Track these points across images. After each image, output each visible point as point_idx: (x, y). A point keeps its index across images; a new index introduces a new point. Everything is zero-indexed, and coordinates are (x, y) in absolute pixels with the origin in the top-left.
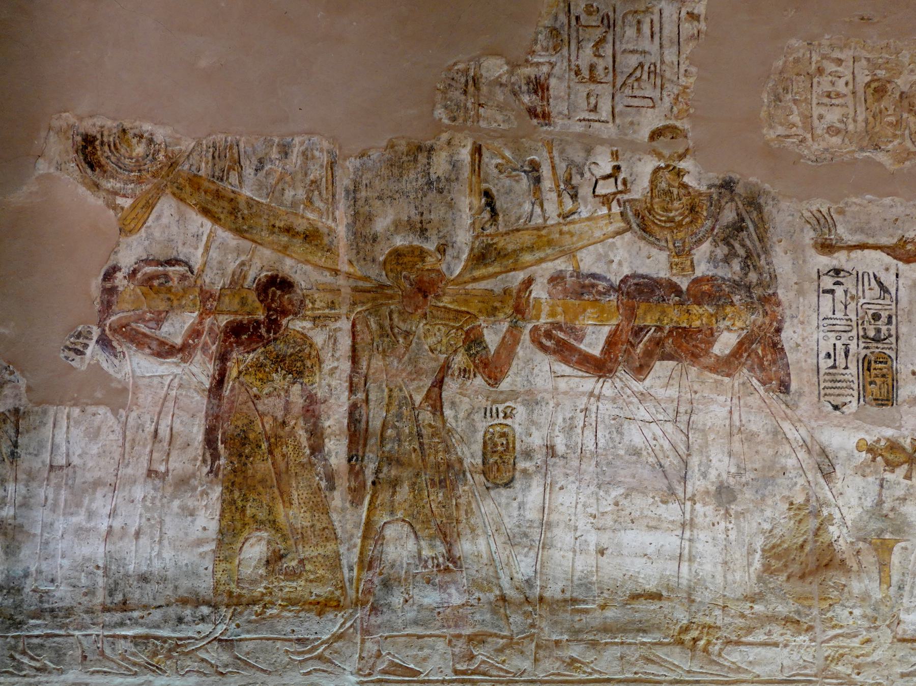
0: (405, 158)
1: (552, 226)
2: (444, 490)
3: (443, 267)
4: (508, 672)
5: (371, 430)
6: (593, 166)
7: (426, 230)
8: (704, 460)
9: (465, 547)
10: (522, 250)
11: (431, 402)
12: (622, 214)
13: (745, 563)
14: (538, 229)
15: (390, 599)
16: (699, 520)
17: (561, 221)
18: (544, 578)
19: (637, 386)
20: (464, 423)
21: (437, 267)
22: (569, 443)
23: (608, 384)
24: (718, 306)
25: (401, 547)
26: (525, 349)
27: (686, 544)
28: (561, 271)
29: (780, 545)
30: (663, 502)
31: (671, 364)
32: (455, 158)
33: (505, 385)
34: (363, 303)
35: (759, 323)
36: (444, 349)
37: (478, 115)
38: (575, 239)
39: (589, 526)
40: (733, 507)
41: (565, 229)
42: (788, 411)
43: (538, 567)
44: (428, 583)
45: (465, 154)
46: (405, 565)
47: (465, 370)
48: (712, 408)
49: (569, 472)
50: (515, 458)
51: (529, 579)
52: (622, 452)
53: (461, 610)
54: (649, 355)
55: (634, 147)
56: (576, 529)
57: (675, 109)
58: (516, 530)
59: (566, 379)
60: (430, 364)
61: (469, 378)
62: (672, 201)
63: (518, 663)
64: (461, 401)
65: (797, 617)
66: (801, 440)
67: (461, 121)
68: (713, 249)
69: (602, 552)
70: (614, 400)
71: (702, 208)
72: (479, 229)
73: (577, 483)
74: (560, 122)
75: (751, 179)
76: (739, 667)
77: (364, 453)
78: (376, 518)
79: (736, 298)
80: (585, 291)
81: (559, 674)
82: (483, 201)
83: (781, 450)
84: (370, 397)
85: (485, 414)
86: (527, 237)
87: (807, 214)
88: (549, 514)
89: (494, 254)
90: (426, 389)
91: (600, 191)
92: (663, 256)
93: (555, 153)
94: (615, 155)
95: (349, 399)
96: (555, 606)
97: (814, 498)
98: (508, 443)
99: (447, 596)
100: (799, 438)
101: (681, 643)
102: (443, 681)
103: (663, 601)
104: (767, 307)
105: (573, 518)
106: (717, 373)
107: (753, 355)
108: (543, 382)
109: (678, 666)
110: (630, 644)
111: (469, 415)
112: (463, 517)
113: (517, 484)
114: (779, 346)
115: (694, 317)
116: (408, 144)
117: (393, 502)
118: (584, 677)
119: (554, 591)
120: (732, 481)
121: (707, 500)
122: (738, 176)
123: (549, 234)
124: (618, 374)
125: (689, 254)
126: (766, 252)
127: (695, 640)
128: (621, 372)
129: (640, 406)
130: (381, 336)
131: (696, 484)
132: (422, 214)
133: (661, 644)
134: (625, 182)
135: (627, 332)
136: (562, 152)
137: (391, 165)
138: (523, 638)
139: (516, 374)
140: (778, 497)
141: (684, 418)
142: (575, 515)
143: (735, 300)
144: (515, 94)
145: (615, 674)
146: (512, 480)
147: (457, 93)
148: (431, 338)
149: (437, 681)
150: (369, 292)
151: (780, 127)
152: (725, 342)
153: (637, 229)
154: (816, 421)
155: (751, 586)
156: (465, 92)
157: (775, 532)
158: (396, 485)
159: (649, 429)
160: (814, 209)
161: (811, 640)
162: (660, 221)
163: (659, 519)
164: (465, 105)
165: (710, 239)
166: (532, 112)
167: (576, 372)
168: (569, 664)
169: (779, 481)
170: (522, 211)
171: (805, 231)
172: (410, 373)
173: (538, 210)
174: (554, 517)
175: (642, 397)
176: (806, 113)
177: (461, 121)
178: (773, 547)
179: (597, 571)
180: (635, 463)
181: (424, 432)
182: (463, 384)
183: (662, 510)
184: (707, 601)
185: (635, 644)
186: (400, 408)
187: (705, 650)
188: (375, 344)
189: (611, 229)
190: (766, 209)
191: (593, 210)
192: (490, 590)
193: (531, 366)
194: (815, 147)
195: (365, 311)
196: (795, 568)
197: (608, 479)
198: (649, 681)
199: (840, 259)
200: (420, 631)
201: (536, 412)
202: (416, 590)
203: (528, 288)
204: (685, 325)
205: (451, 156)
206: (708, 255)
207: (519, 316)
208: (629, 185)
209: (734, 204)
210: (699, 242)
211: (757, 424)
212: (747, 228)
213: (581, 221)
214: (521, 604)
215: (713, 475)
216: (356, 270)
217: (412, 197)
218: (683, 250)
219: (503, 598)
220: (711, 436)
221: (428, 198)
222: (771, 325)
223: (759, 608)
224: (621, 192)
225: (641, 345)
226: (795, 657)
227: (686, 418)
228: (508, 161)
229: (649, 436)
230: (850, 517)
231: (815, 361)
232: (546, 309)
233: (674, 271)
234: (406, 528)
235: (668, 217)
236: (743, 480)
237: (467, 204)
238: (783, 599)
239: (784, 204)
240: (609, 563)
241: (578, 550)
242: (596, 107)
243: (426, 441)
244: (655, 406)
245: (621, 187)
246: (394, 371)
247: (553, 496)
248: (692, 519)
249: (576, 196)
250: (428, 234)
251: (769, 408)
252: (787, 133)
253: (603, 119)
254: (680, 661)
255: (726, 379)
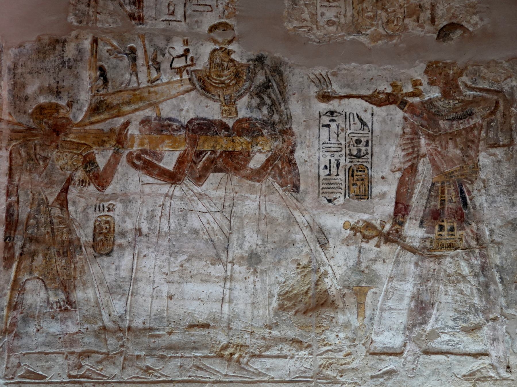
0: (47, 47)
1: (144, 88)
2: (66, 258)
3: (71, 116)
4: (104, 376)
5: (20, 220)
6: (171, 49)
7: (60, 92)
8: (241, 236)
9: (78, 295)
10: (123, 103)
11: (60, 202)
12: (190, 79)
13: (267, 303)
14: (134, 90)
15: (28, 329)
16: (236, 276)
17: (149, 84)
18: (132, 314)
19: (198, 189)
20: (81, 215)
21: (67, 116)
22: (150, 227)
23: (178, 188)
24: (253, 137)
25: (36, 295)
26: (123, 167)
27: (227, 291)
28: (148, 117)
29: (291, 292)
30: (212, 264)
31: (221, 175)
32: (80, 47)
33: (109, 190)
34: (17, 140)
35: (280, 147)
36: (69, 167)
37: (96, 19)
38: (158, 96)
39: (163, 280)
40: (259, 267)
41: (152, 90)
42: (298, 204)
43: (128, 308)
44: (53, 318)
45: (87, 44)
46: (38, 307)
47: (83, 181)
48: (247, 202)
49: (150, 245)
50: (114, 237)
51: (122, 315)
52: (186, 232)
53: (75, 336)
54: (206, 169)
55: (198, 36)
56: (154, 282)
57: (226, 12)
58: (114, 283)
59: (150, 186)
60: (59, 177)
61: (85, 186)
62: (223, 70)
63: (112, 370)
64: (79, 201)
65: (300, 339)
66: (306, 223)
67: (85, 23)
68: (250, 100)
69: (171, 297)
70: (181, 199)
71: (243, 74)
72: (95, 91)
73: (155, 253)
74: (150, 22)
75: (275, 55)
76: (260, 372)
77: (14, 235)
78: (20, 277)
79: (265, 132)
80: (164, 129)
81: (138, 378)
82: (98, 73)
83: (292, 229)
84: (20, 199)
85: (95, 209)
86: (126, 95)
87: (312, 77)
88: (136, 273)
89: (104, 107)
90: (57, 194)
91: (174, 65)
92: (217, 106)
93: (147, 42)
94: (186, 42)
95: (7, 201)
96: (138, 333)
97: (315, 261)
98: (110, 228)
99: (65, 327)
100: (305, 221)
101: (221, 356)
102: (61, 383)
103: (210, 329)
104: (285, 137)
105: (152, 275)
106: (252, 180)
107: (275, 168)
108: (134, 188)
109: (218, 372)
110: (187, 357)
111: (85, 209)
112: (78, 276)
113: (115, 254)
114: (293, 162)
115: (237, 144)
116: (50, 39)
117: (31, 266)
118: (155, 379)
119: (138, 323)
120: (259, 250)
121: (242, 262)
122: (267, 53)
123: (141, 93)
124: (185, 182)
125: (234, 103)
126: (285, 101)
127: (232, 354)
128: (186, 181)
129: (199, 202)
130: (28, 160)
131: (235, 251)
132: (58, 82)
133: (207, 357)
134: (192, 59)
135: (192, 155)
136: (151, 41)
137: (39, 52)
138: (116, 354)
139: (117, 183)
140: (289, 260)
141: (228, 210)
142: (154, 273)
143: (264, 133)
144: (121, 5)
145: (176, 377)
146: (112, 251)
147: (83, 6)
148: (61, 160)
149: (57, 383)
150: (22, 132)
151: (295, 22)
152: (257, 160)
153: (199, 88)
154: (316, 210)
155: (270, 318)
156: (89, 5)
157: (287, 283)
158: (34, 255)
159: (205, 217)
160: (317, 73)
161: (310, 354)
162: (215, 83)
163: (209, 275)
164: (88, 13)
165: (248, 94)
166: (132, 16)
167: (157, 181)
168: (145, 371)
169: (290, 249)
170: (124, 79)
171: (311, 87)
172: (47, 183)
173: (134, 78)
174: (140, 275)
175: (200, 196)
176: (313, 12)
177: (85, 23)
178: (287, 293)
179: (167, 310)
180: (195, 239)
181: (54, 221)
182: (82, 190)
183: (212, 270)
184: (240, 328)
185: (191, 357)
186: (39, 205)
187: (238, 361)
188: (24, 165)
189: (182, 89)
190: (285, 74)
191: (170, 77)
192: (96, 323)
193: (126, 178)
194: (319, 33)
195: (18, 144)
196: (301, 307)
197: (176, 250)
198: (199, 382)
199: (334, 105)
200: (47, 350)
201: (129, 207)
202: (45, 323)
203: (126, 127)
204: (231, 149)
205: (78, 46)
206: (246, 103)
207: (120, 146)
208: (194, 61)
209: (264, 71)
210: (241, 96)
211: (277, 212)
212: (272, 86)
213: (163, 84)
214: (116, 332)
215: (246, 246)
216: (14, 119)
217: (52, 72)
218: (230, 102)
219: (104, 328)
220: (246, 221)
221: (62, 72)
222: (287, 148)
223: (275, 333)
224: (189, 65)
225: (201, 163)
226: (298, 365)
227: (229, 209)
228: (116, 48)
229: (205, 222)
230: (339, 272)
231: (317, 171)
232: (137, 141)
233: (224, 115)
234: (40, 283)
235: (220, 81)
236: (267, 249)
237: (87, 76)
238: (291, 327)
239: (297, 71)
240: (175, 305)
241: (155, 296)
242: (173, 12)
243: (56, 227)
244: (209, 202)
245: (189, 62)
246: (36, 183)
247: (139, 261)
248: (231, 275)
249: (159, 68)
250: (61, 95)
251: (285, 202)
252: (301, 25)
253: (178, 19)
254: (221, 369)
255: (257, 184)
